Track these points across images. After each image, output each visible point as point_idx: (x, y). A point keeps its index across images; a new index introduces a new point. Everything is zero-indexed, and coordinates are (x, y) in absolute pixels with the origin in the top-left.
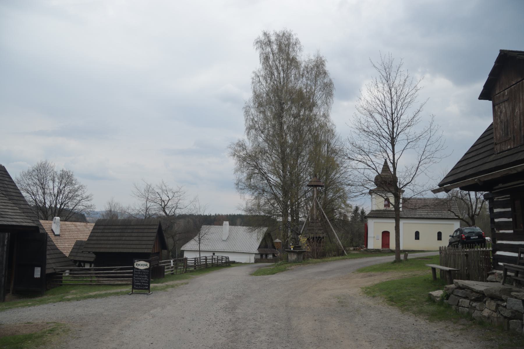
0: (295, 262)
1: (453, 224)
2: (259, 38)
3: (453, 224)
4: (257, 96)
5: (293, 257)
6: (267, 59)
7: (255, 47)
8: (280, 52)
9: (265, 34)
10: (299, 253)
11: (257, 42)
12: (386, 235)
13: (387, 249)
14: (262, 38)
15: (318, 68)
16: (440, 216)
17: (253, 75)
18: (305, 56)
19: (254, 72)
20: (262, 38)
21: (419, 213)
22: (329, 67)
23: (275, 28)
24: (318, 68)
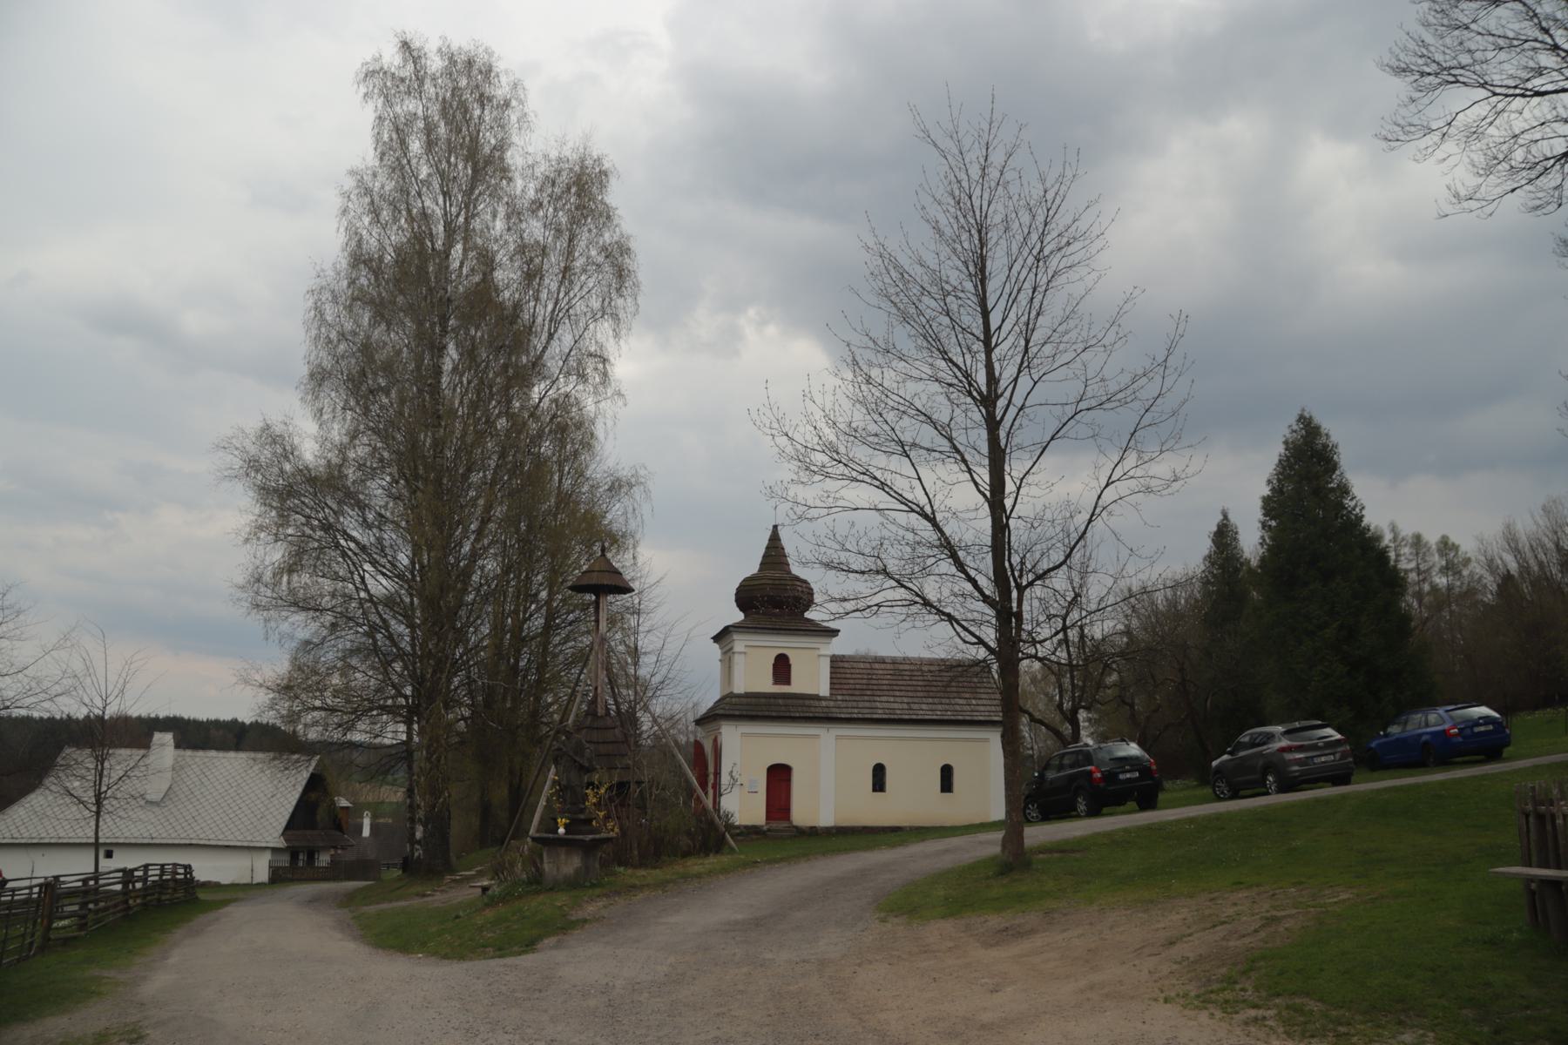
0: (573, 884)
1: (987, 740)
2: (378, 59)
3: (987, 740)
4: (359, 259)
5: (571, 864)
6: (401, 132)
7: (363, 90)
8: (449, 122)
9: (405, 45)
10: (588, 849)
11: (370, 74)
12: (779, 776)
13: (784, 824)
14: (392, 58)
15: (580, 190)
16: (949, 716)
17: (349, 183)
18: (536, 143)
19: (352, 173)
20: (392, 58)
21: (886, 704)
22: (615, 196)
23: (443, 29)
24: (580, 190)
